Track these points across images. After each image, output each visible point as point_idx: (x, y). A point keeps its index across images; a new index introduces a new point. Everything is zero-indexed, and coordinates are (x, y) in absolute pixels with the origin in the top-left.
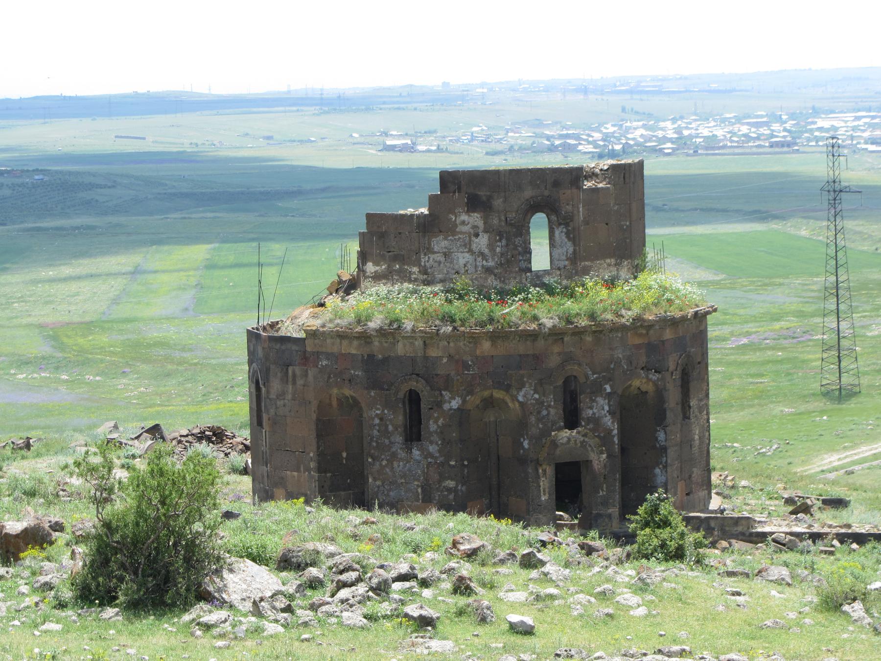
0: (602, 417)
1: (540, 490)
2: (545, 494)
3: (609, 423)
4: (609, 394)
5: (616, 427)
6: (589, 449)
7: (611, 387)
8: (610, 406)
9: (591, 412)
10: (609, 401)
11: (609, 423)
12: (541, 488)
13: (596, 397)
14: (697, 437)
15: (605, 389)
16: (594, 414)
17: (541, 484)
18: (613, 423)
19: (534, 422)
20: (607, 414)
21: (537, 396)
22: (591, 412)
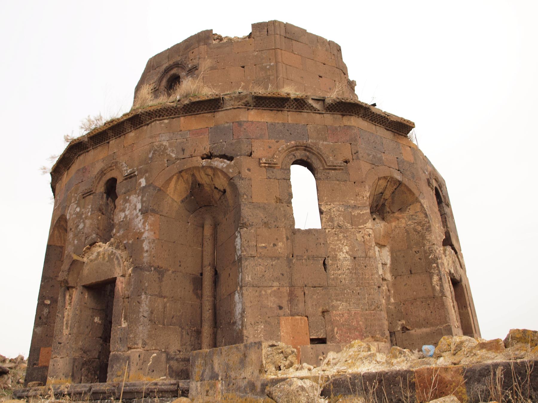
0: (133, 219)
1: (63, 323)
2: (67, 328)
3: (140, 225)
4: (144, 187)
5: (147, 228)
6: (116, 262)
7: (147, 180)
8: (142, 202)
9: (122, 215)
10: (142, 197)
11: (140, 225)
12: (65, 320)
13: (129, 196)
14: (341, 256)
15: (140, 184)
16: (126, 217)
17: (66, 314)
18: (144, 223)
19: (71, 240)
20: (139, 214)
21: (78, 210)
22: (122, 215)
